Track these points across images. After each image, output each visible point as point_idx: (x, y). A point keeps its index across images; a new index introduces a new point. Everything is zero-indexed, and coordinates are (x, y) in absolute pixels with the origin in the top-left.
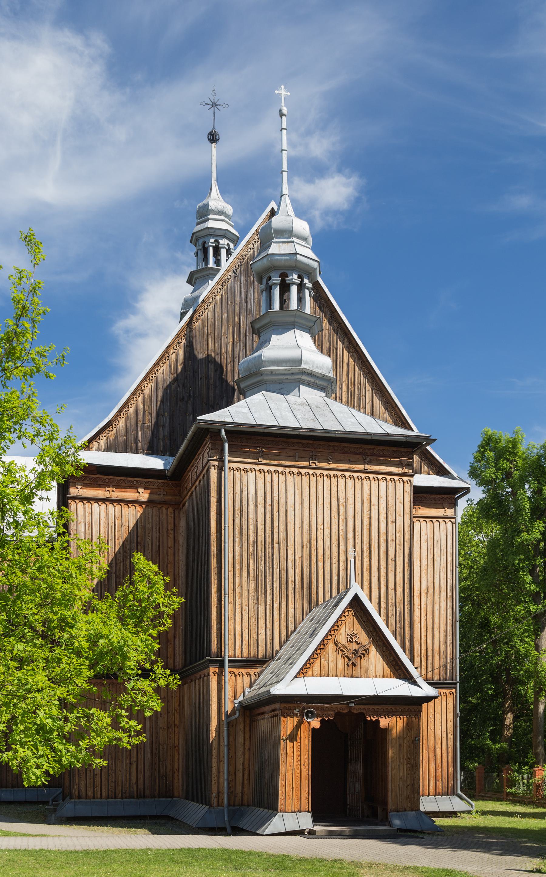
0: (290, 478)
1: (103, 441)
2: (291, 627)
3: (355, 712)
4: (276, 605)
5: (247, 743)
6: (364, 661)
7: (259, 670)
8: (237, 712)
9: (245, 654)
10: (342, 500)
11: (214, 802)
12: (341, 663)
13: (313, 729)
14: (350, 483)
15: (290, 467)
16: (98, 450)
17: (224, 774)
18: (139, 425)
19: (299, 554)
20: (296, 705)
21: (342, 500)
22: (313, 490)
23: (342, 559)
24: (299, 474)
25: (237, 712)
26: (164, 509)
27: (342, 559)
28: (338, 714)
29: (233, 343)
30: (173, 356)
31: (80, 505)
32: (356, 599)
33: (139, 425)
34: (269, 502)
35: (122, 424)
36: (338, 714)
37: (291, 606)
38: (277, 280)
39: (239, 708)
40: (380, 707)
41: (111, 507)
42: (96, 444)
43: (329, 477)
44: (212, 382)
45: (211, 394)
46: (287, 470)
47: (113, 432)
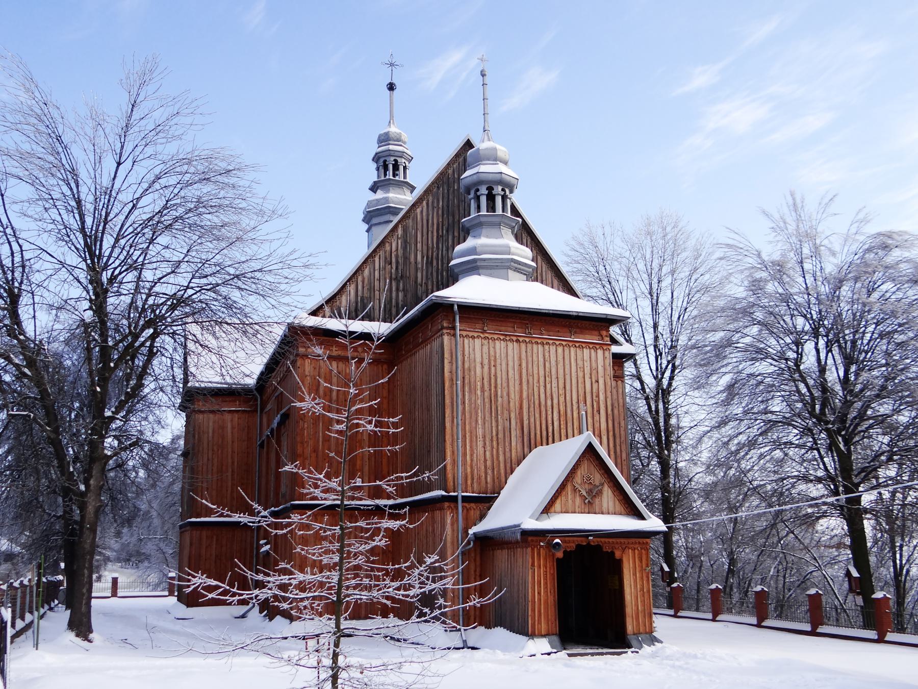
0: (510, 344)
3: (592, 544)
5: (478, 570)
6: (597, 501)
8: (472, 542)
12: (578, 500)
13: (558, 559)
14: (560, 349)
15: (510, 335)
16: (324, 316)
17: (459, 598)
18: (359, 298)
20: (541, 538)
22: (529, 354)
24: (518, 341)
25: (472, 542)
26: (380, 368)
28: (578, 546)
29: (437, 237)
32: (590, 448)
33: (359, 298)
36: (578, 546)
39: (474, 538)
40: (614, 540)
43: (543, 344)
44: (420, 266)
45: (419, 275)
46: (508, 338)
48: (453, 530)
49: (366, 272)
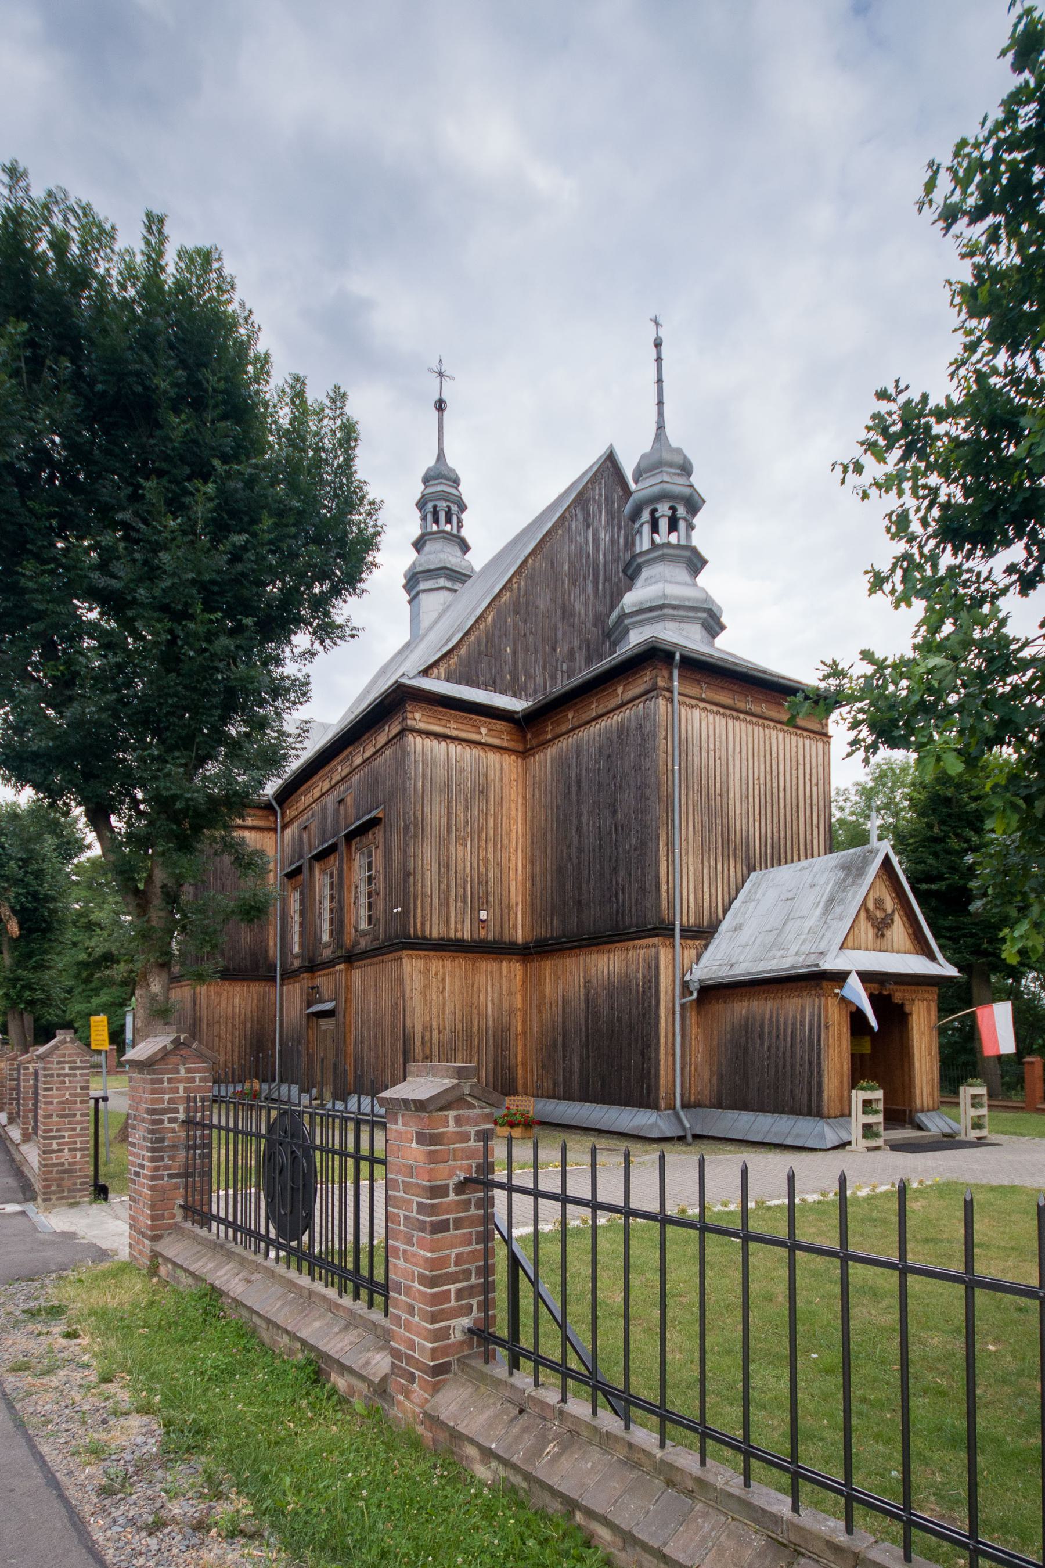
1: (442, 669)
2: (733, 892)
4: (719, 867)
7: (703, 942)
9: (692, 921)
10: (774, 755)
11: (662, 1104)
19: (738, 812)
21: (774, 755)
23: (775, 820)
27: (775, 820)
30: (515, 586)
31: (419, 740)
34: (711, 747)
35: (463, 651)
37: (732, 870)
38: (663, 509)
41: (452, 746)
42: (436, 671)
47: (454, 660)
48: (667, 977)
49: (490, 619)
